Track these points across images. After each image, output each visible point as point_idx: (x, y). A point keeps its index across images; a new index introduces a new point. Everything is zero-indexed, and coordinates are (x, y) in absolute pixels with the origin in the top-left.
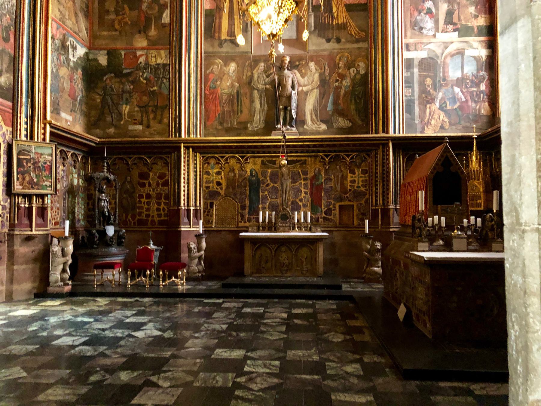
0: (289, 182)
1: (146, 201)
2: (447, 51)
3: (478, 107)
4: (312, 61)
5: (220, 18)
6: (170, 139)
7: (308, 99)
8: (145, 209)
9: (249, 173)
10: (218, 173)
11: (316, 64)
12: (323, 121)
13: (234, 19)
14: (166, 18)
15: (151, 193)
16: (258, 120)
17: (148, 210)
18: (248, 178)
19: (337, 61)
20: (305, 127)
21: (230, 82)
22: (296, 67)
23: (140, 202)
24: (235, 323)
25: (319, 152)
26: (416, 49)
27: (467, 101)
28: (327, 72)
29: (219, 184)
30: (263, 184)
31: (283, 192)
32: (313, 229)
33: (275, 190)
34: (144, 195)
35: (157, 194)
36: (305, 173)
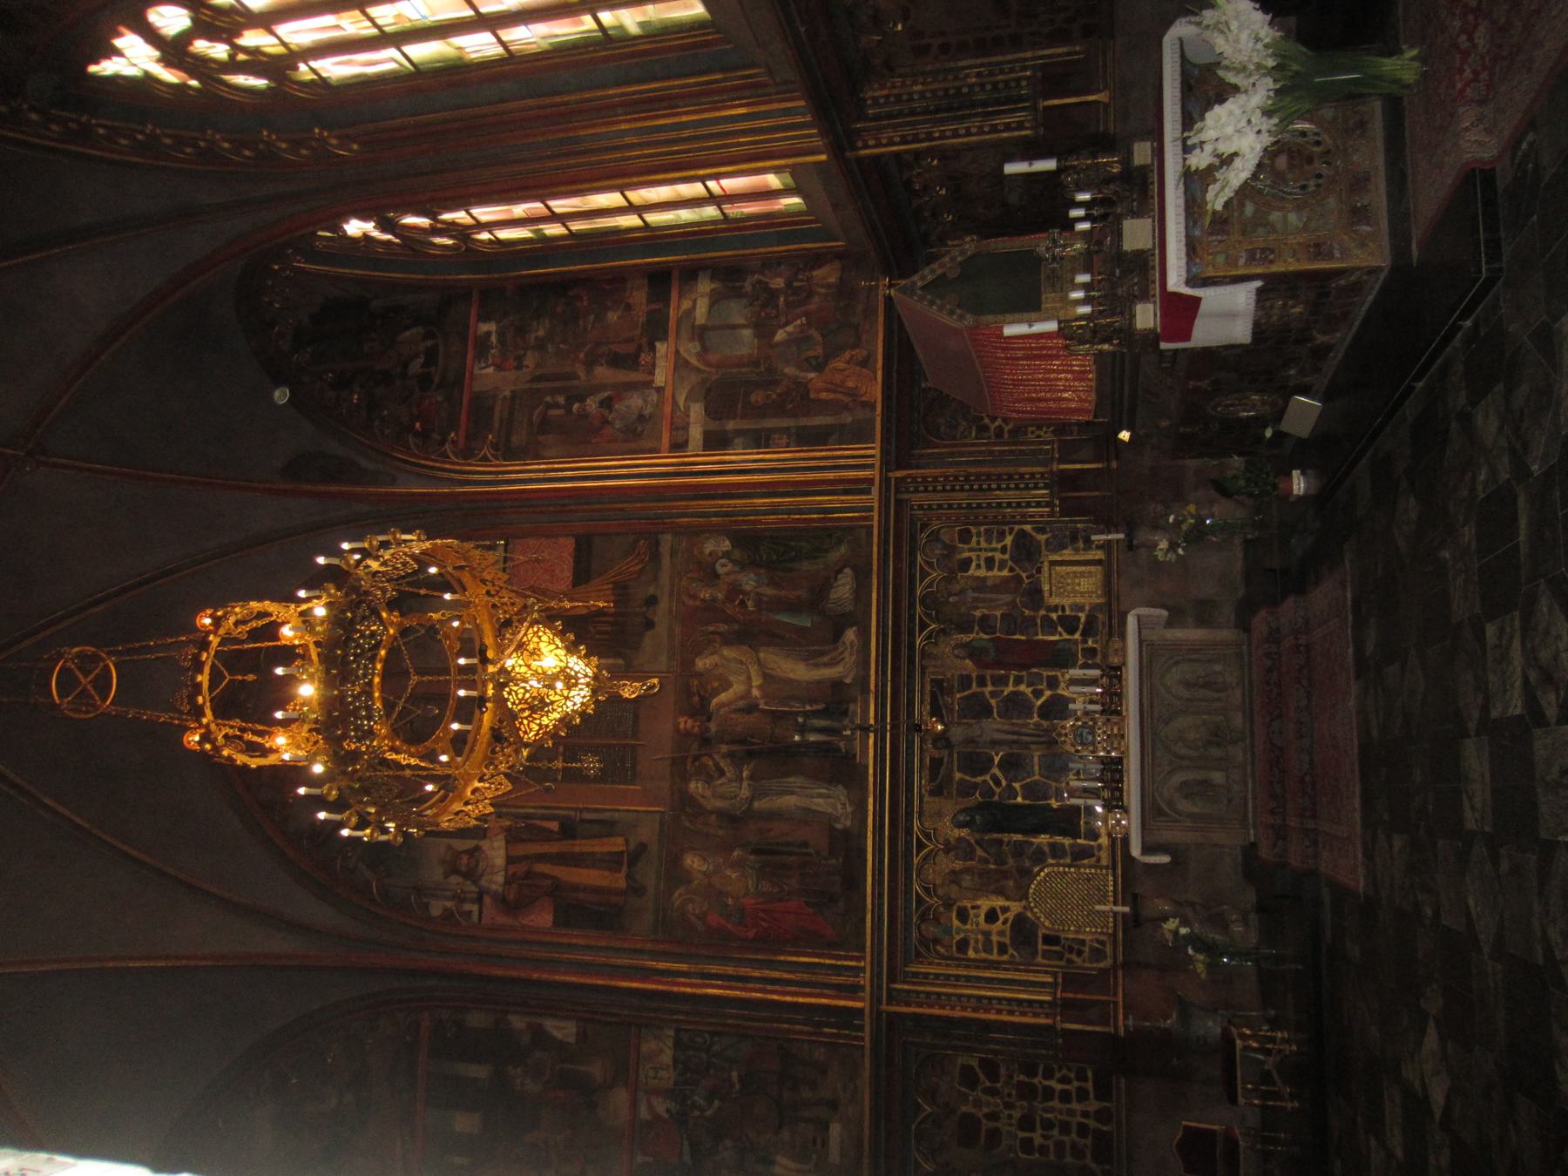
0: (987, 724)
1: (1039, 1131)
2: (694, 361)
3: (822, 291)
4: (693, 663)
5: (576, 888)
6: (867, 1043)
7: (781, 674)
8: (1065, 1138)
9: (964, 832)
10: (963, 916)
11: (699, 654)
12: (837, 635)
13: (582, 854)
14: (563, 1030)
15: (1017, 1114)
16: (828, 801)
17: (1065, 1128)
18: (978, 836)
19: (698, 603)
20: (848, 681)
21: (728, 872)
22: (705, 701)
23: (1043, 1150)
24: (1386, 817)
25: (911, 646)
26: (686, 427)
27: (807, 314)
28: (723, 628)
29: (992, 916)
30: (994, 793)
31: (1014, 742)
32: (1115, 661)
33: (1012, 765)
34: (1022, 1134)
35: (1021, 1097)
36: (965, 681)
